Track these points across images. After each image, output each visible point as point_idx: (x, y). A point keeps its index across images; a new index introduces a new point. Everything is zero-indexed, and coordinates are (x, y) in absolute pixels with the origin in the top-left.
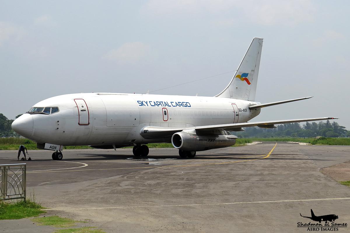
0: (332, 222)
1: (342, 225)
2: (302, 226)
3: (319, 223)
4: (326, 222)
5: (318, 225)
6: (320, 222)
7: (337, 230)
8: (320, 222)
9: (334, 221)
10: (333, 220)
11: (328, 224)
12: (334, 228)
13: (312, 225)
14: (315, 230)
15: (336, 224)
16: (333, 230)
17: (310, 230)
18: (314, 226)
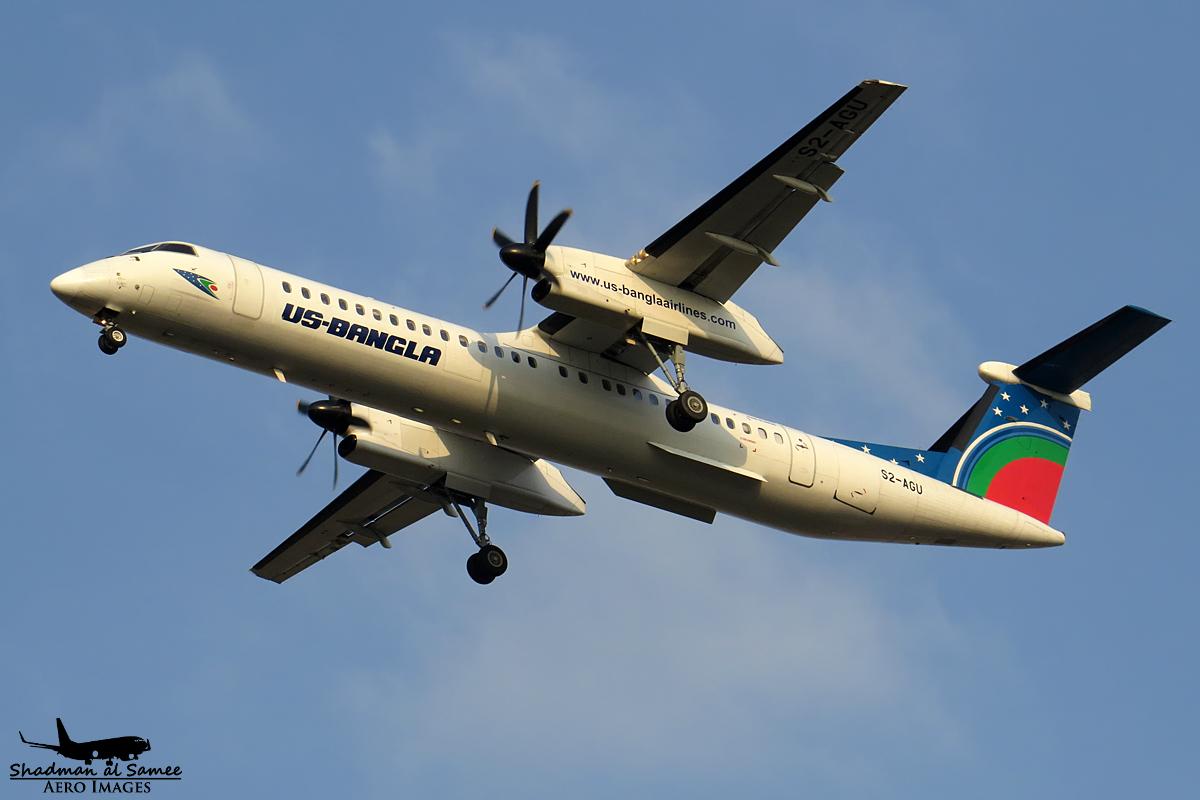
0: (128, 763)
1: (164, 771)
2: (27, 775)
3: (85, 767)
4: (110, 763)
5: (81, 772)
6: (90, 763)
7: (147, 790)
8: (88, 762)
9: (136, 758)
10: (131, 756)
11: (115, 771)
12: (137, 784)
13: (60, 771)
14: (72, 788)
15: (142, 770)
16: (132, 789)
17: (55, 790)
18: (69, 775)
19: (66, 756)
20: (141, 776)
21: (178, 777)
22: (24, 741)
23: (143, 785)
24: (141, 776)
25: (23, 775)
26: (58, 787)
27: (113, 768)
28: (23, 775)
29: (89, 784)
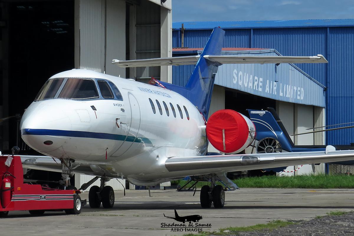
0: (196, 223)
2: (166, 226)
4: (190, 223)
5: (182, 225)
8: (184, 223)
9: (198, 221)
10: (197, 221)
11: (192, 225)
13: (175, 225)
14: (179, 230)
15: (200, 225)
17: (174, 231)
18: (178, 226)
19: (177, 221)
20: (199, 227)
22: (165, 216)
24: (199, 227)
25: (165, 226)
28: (165, 226)
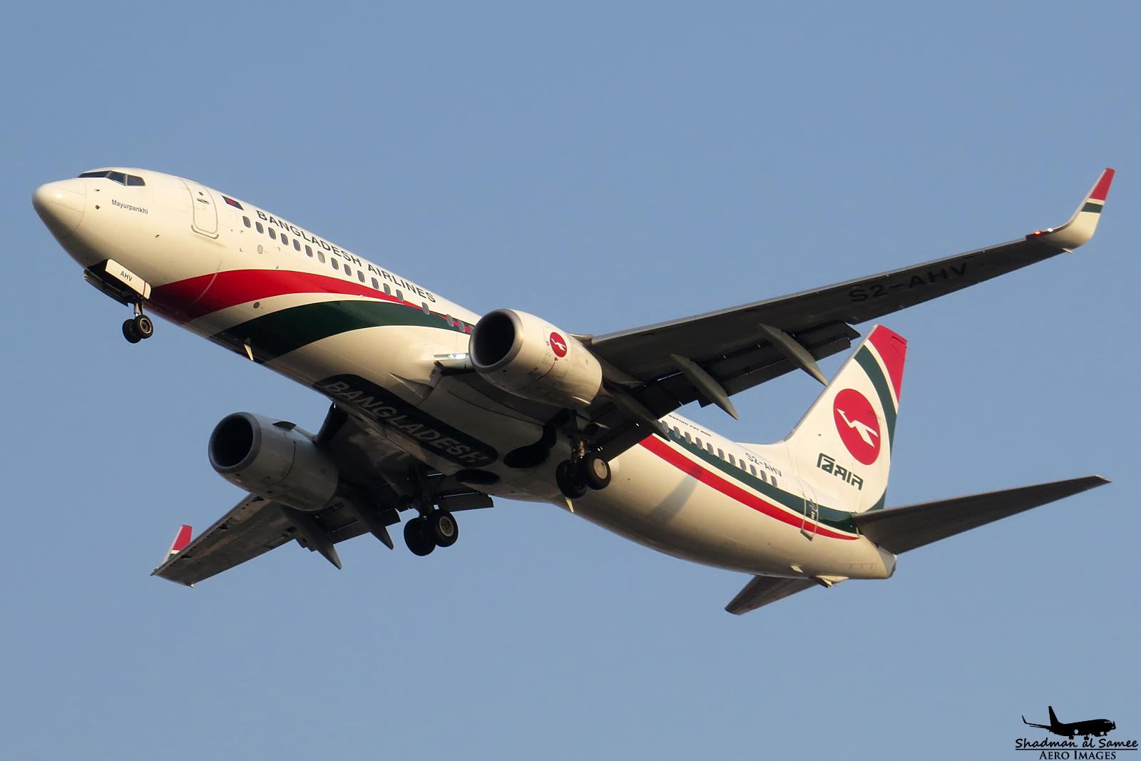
0: (1100, 738)
2: (1027, 747)
4: (1086, 738)
5: (1066, 744)
7: (1113, 757)
8: (1071, 738)
9: (1105, 734)
10: (1102, 733)
11: (1091, 744)
14: (1060, 756)
15: (1110, 743)
16: (1102, 757)
17: (1047, 757)
18: (1057, 747)
20: (1109, 748)
21: (1136, 748)
22: (1025, 722)
23: (1111, 756)
24: (1109, 748)
25: (1025, 746)
26: (1050, 755)
27: (1089, 742)
28: (1025, 746)
29: (1072, 753)
